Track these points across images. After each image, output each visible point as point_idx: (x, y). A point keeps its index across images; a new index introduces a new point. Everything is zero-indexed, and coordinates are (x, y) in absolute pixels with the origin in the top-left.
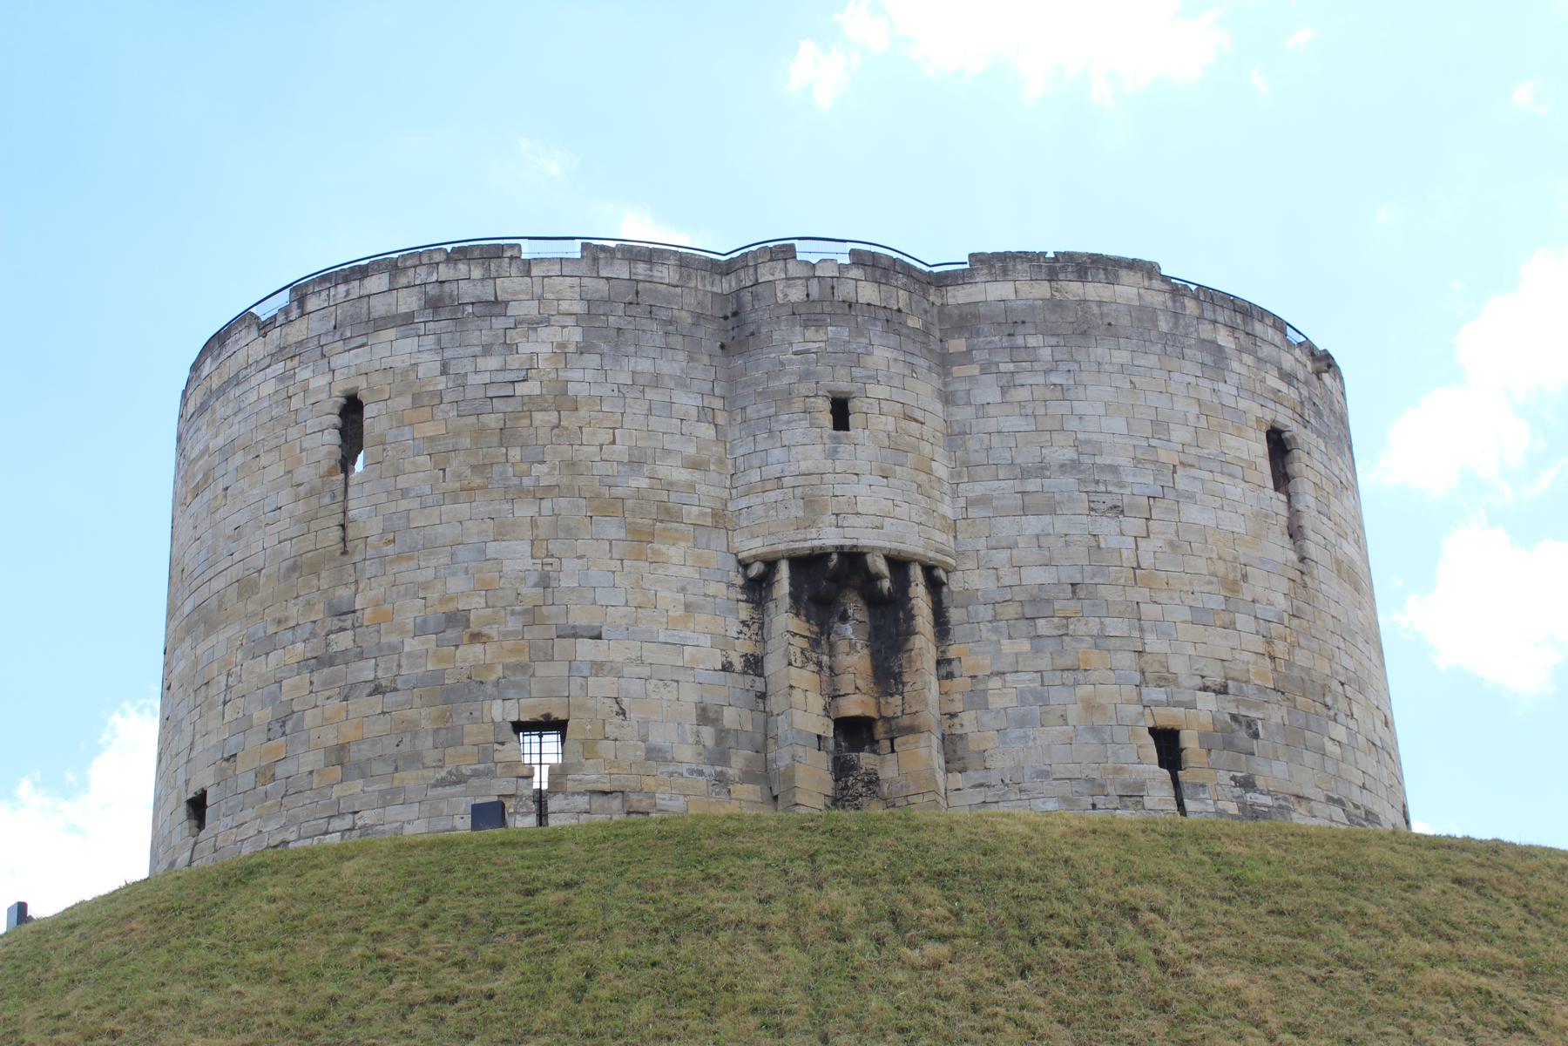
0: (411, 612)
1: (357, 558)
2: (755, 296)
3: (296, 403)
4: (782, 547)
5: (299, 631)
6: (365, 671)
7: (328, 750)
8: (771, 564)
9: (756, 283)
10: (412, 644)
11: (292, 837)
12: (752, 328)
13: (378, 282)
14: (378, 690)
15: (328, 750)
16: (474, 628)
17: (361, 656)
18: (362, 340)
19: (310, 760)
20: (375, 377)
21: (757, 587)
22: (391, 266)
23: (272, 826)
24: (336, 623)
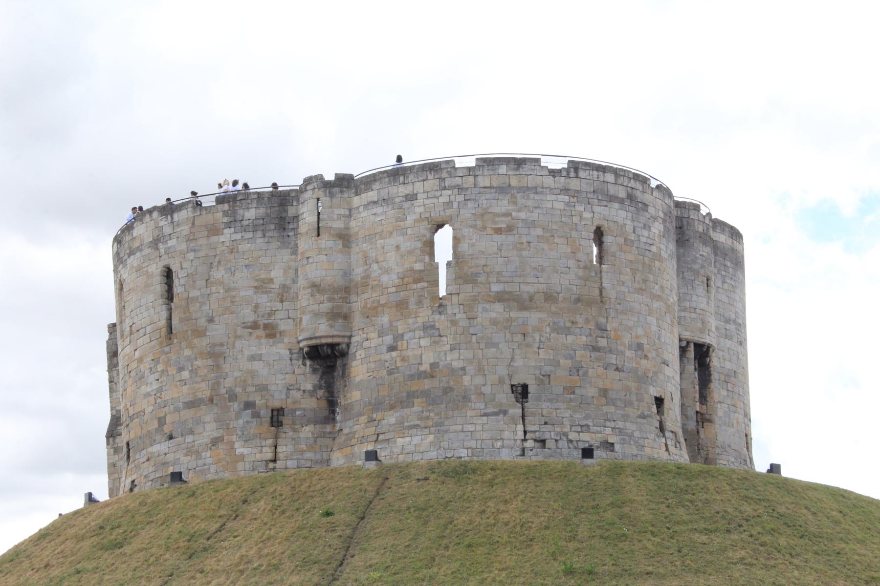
0: (627, 339)
1: (607, 307)
2: (688, 223)
3: (576, 219)
4: (696, 339)
5: (583, 331)
6: (612, 359)
7: (600, 390)
8: (688, 343)
9: (689, 218)
10: (628, 353)
11: (591, 424)
12: (687, 238)
13: (610, 177)
14: (617, 369)
15: (600, 390)
16: (645, 353)
17: (611, 351)
18: (605, 203)
19: (592, 392)
20: (612, 224)
21: (683, 350)
22: (618, 173)
23: (577, 416)
24: (599, 333)
